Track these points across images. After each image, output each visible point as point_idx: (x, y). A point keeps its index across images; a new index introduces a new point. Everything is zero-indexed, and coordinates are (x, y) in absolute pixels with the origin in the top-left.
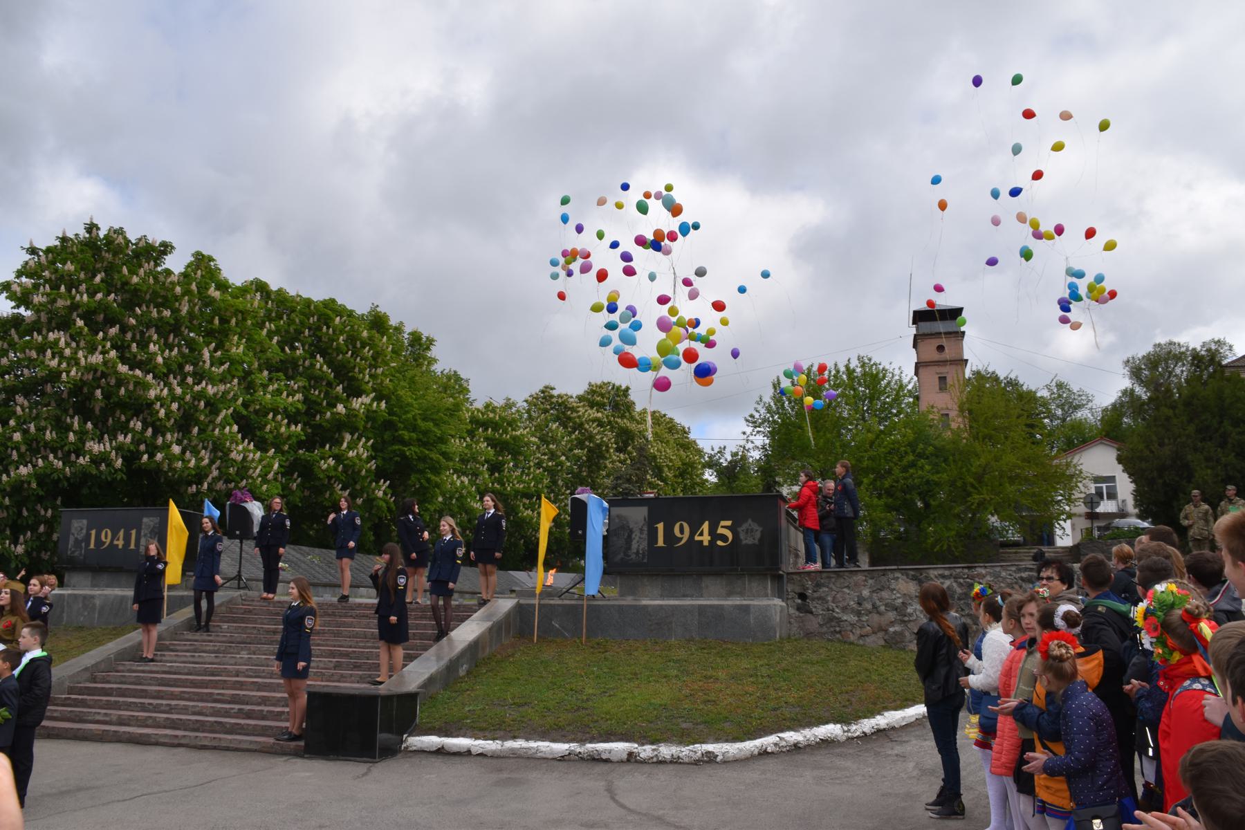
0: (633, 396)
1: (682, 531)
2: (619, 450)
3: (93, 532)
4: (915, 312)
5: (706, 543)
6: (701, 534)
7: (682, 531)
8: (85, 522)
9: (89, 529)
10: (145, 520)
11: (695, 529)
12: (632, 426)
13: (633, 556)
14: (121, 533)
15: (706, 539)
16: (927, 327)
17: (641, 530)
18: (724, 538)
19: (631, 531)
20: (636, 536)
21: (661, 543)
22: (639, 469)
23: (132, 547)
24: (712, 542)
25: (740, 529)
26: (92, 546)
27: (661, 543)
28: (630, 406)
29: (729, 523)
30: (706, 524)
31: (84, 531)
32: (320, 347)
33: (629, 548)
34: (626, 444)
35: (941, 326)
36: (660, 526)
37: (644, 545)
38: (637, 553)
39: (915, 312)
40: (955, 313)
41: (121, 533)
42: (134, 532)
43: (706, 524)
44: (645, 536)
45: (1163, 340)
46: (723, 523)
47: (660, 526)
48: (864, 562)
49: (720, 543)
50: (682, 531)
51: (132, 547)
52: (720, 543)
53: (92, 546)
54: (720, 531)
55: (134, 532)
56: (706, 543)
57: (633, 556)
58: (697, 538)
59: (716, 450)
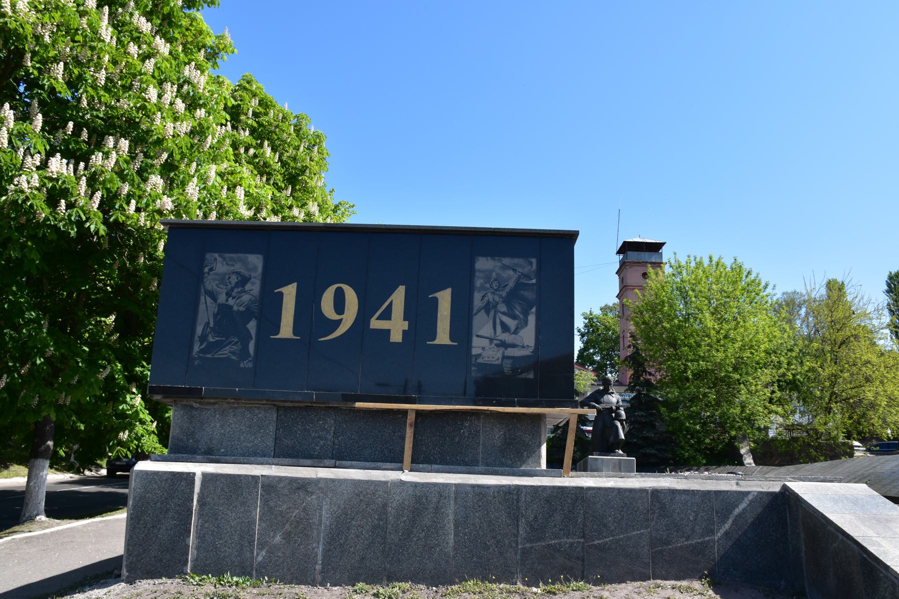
3: (290, 292)
8: (256, 261)
9: (272, 282)
10: (483, 264)
14: (398, 298)
16: (633, 256)
23: (443, 337)
26: (286, 330)
31: (254, 288)
32: (260, 133)
35: (645, 256)
40: (656, 247)
41: (398, 298)
42: (445, 298)
45: (790, 290)
48: (749, 460)
51: (443, 337)
53: (286, 330)
55: (445, 298)
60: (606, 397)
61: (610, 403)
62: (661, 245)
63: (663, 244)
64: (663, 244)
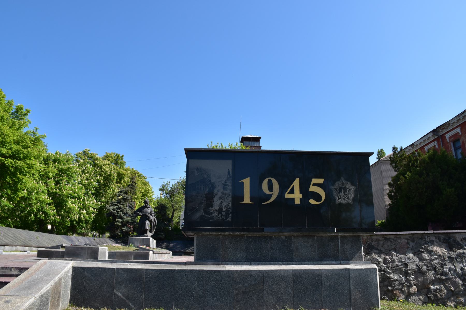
0: (125, 159)
1: (271, 188)
2: (117, 182)
4: (242, 137)
5: (297, 202)
6: (292, 192)
7: (271, 189)
11: (285, 185)
12: (124, 172)
13: (215, 214)
15: (297, 197)
17: (224, 185)
18: (317, 197)
19: (213, 186)
20: (218, 191)
21: (247, 200)
22: (131, 188)
24: (305, 199)
25: (332, 188)
27: (247, 200)
28: (123, 164)
29: (321, 181)
30: (297, 180)
33: (210, 205)
34: (121, 180)
36: (247, 182)
37: (227, 203)
38: (220, 211)
39: (242, 137)
43: (297, 180)
44: (229, 191)
46: (315, 181)
47: (247, 182)
49: (312, 202)
50: (271, 188)
52: (312, 202)
54: (312, 189)
56: (297, 202)
57: (215, 214)
58: (288, 196)
59: (166, 183)
60: (145, 209)
61: (147, 212)
62: (260, 138)
63: (260, 138)
64: (260, 138)
